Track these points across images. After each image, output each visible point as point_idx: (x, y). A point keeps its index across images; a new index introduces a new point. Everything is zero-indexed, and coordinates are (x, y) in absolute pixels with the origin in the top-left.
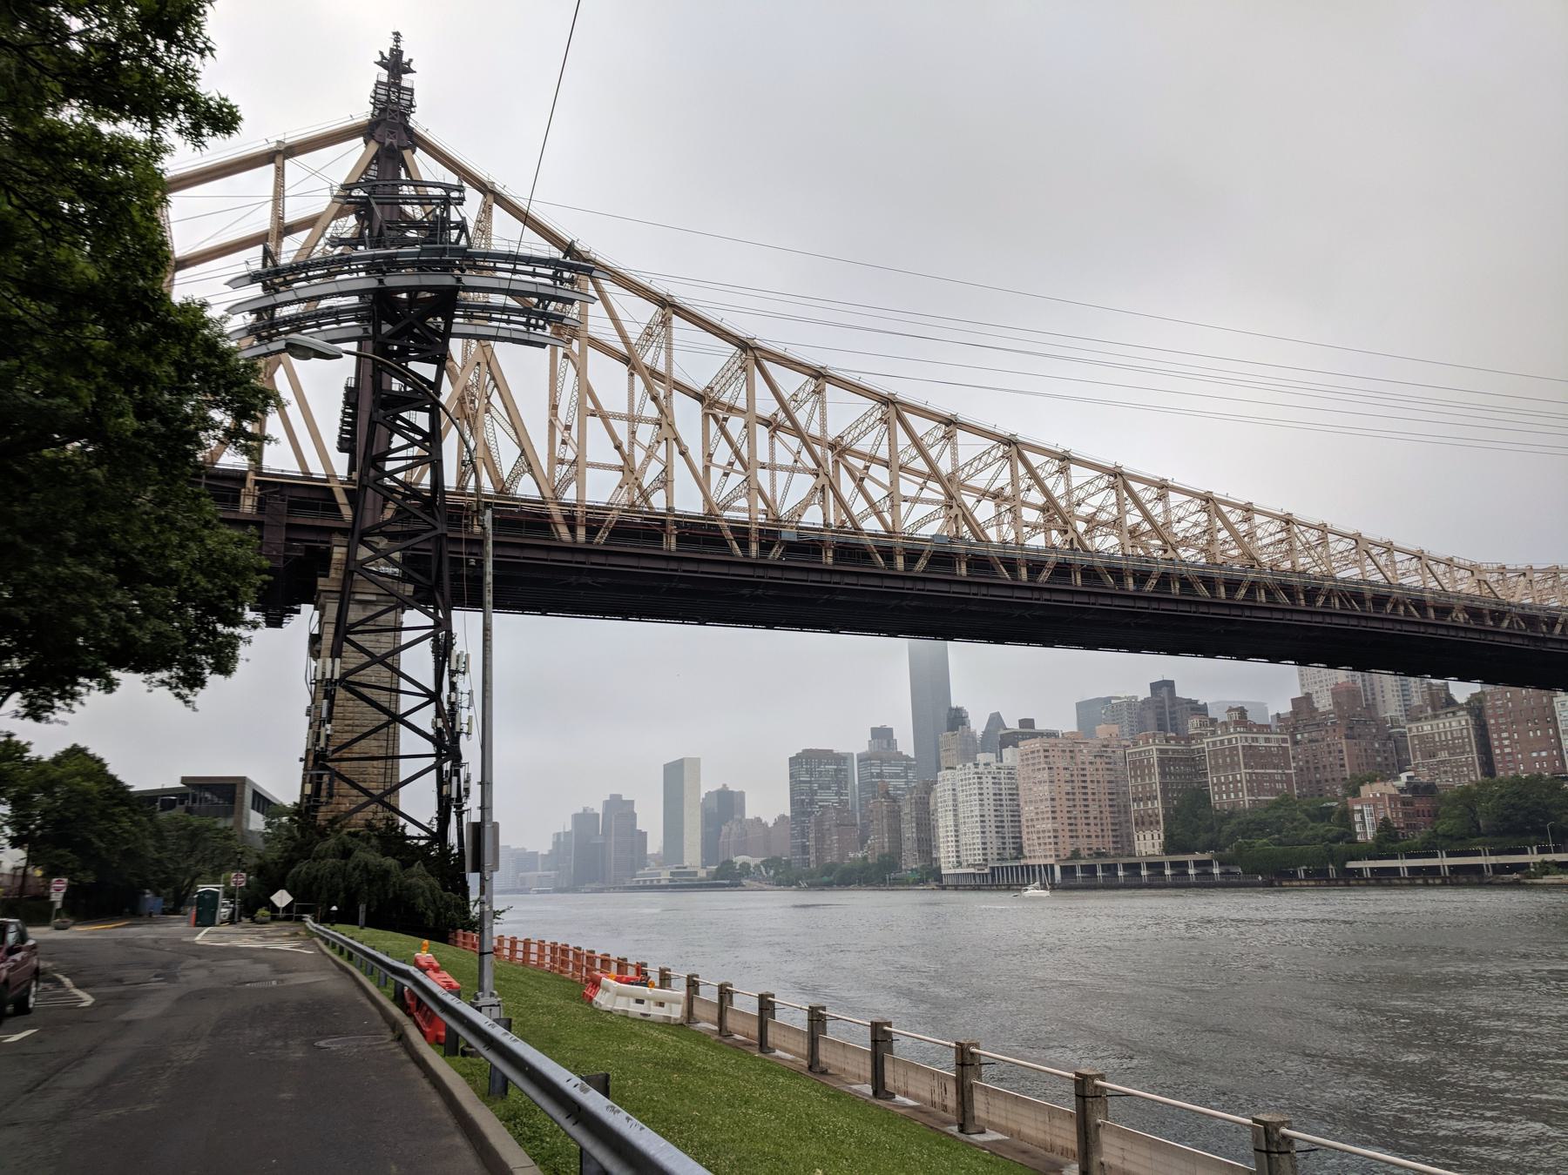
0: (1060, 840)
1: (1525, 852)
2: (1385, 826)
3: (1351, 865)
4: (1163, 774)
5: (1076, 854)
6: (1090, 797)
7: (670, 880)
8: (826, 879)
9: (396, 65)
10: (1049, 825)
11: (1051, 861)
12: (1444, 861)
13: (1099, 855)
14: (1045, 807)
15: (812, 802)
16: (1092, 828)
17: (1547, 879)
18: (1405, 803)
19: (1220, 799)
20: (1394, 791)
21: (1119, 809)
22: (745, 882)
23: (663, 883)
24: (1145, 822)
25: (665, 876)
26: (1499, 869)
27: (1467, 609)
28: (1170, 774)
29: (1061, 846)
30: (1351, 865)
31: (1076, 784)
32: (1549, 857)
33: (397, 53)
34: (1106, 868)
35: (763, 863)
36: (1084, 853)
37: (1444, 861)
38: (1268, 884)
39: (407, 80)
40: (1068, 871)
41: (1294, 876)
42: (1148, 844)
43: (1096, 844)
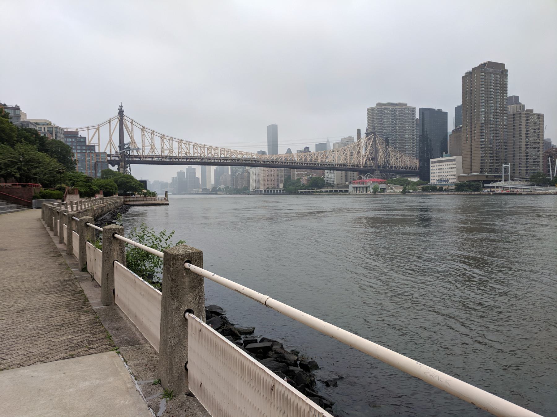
0: (265, 185)
1: (314, 189)
2: (303, 184)
3: (298, 191)
4: (284, 172)
5: (268, 188)
6: (272, 176)
7: (202, 192)
8: (234, 192)
9: (121, 106)
10: (262, 182)
11: (263, 189)
12: (307, 191)
13: (273, 188)
14: (262, 178)
15: (236, 172)
16: (272, 182)
17: (314, 194)
18: (308, 180)
19: (292, 178)
20: (307, 178)
21: (278, 178)
22: (218, 192)
23: (200, 192)
24: (281, 182)
25: (200, 191)
26: (312, 192)
27: (263, 161)
28: (286, 172)
29: (265, 186)
30: (298, 191)
31: (270, 174)
32: (316, 190)
33: (121, 105)
34: (274, 191)
35: (225, 188)
36: (270, 188)
37: (307, 191)
38: (289, 194)
39: (123, 109)
40: (265, 191)
41: (292, 193)
42: (281, 186)
43: (273, 186)
